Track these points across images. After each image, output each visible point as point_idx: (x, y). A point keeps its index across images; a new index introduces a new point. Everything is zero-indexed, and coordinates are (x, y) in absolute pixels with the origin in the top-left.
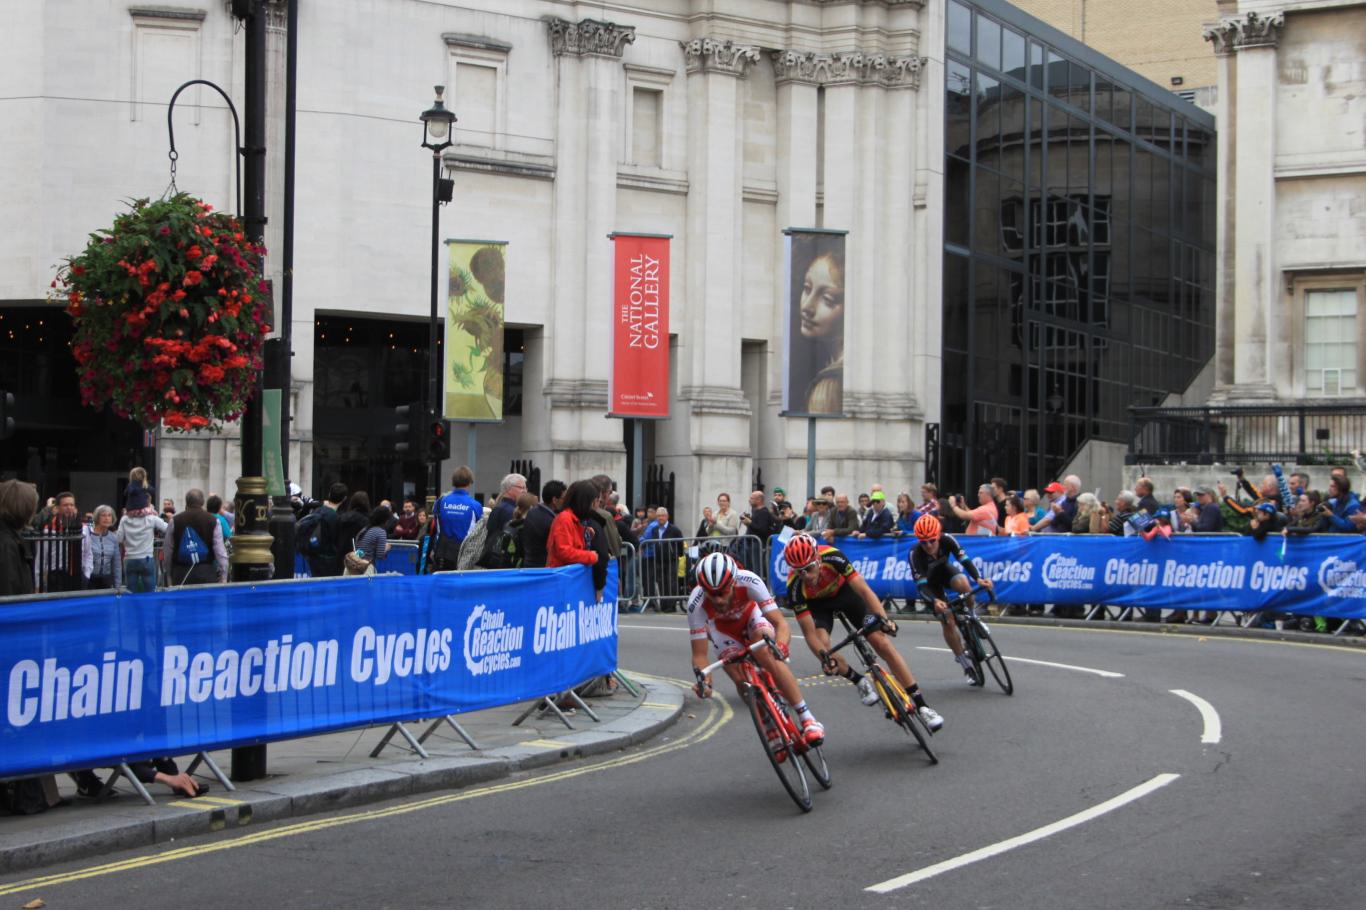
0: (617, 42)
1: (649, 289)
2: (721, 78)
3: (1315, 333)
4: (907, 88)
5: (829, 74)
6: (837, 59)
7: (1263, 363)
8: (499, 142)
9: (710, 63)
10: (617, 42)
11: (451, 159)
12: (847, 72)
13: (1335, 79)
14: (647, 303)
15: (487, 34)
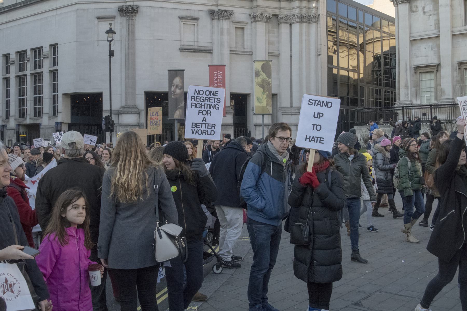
0: (229, 15)
1: (219, 80)
2: (260, 23)
3: (424, 84)
4: (314, 23)
5: (292, 20)
6: (294, 16)
7: (408, 94)
8: (196, 44)
9: (256, 19)
10: (229, 15)
11: (181, 49)
12: (297, 19)
13: (426, 10)
14: (219, 84)
15: (192, 16)
